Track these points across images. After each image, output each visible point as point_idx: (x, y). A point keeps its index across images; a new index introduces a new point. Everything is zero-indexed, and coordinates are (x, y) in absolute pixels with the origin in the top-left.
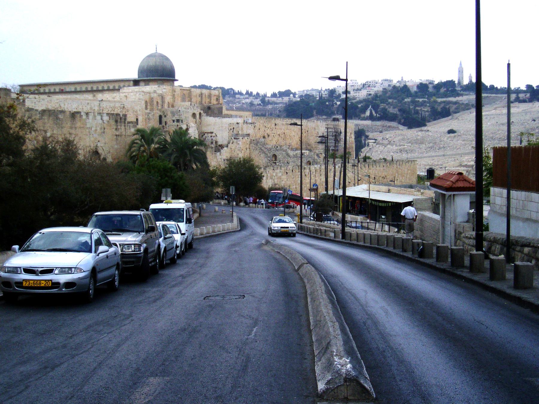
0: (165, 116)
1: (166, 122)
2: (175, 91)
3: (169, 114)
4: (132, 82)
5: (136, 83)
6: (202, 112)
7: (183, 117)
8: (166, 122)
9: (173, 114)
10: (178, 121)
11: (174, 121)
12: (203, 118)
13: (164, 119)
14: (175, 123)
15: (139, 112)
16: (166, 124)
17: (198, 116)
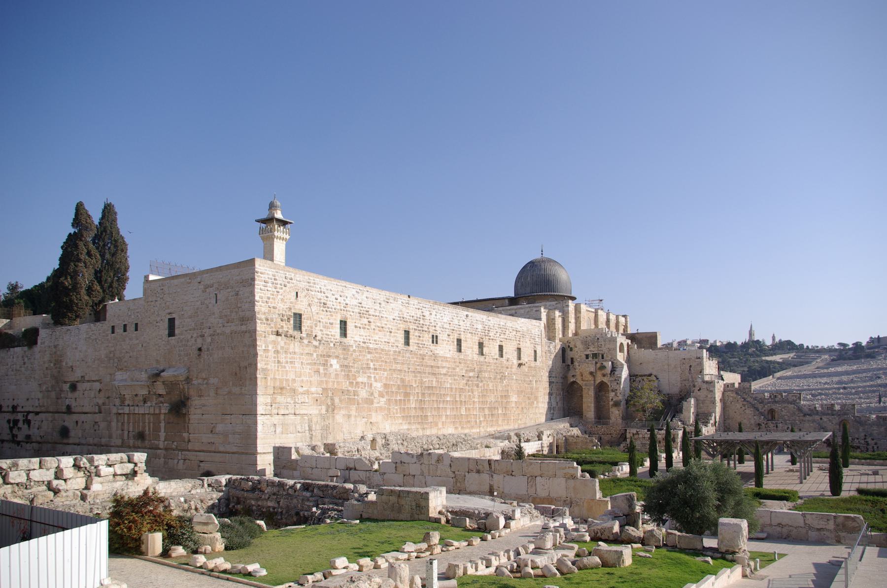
0: (571, 350)
1: (572, 359)
2: (580, 312)
3: (580, 345)
4: (507, 301)
5: (513, 301)
6: (629, 341)
7: (604, 350)
9: (586, 344)
10: (595, 356)
11: (587, 356)
12: (632, 352)
13: (570, 354)
14: (590, 359)
15: (537, 340)
16: (572, 362)
17: (626, 349)
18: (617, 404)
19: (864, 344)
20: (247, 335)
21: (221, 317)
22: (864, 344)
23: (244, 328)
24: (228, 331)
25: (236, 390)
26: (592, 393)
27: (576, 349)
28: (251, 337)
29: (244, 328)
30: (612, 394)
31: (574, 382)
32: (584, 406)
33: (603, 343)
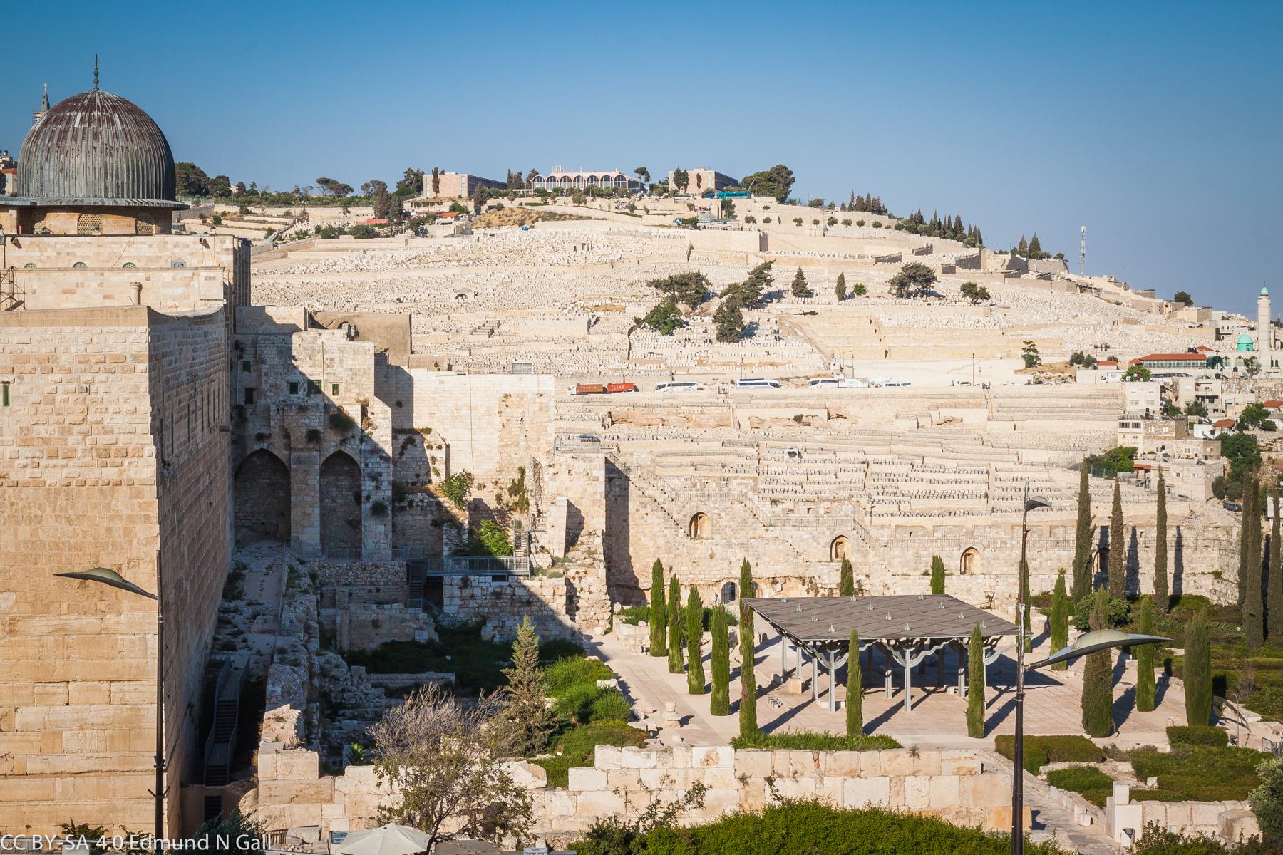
8: (249, 393)
18: (378, 510)
19: (392, 189)
20: (124, 491)
21: (25, 444)
22: (392, 189)
23: (111, 473)
24: (54, 477)
25: (90, 622)
26: (314, 481)
27: (265, 368)
28: (138, 494)
29: (111, 473)
30: (368, 486)
31: (263, 452)
32: (295, 513)
33: (337, 356)
